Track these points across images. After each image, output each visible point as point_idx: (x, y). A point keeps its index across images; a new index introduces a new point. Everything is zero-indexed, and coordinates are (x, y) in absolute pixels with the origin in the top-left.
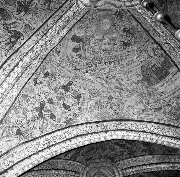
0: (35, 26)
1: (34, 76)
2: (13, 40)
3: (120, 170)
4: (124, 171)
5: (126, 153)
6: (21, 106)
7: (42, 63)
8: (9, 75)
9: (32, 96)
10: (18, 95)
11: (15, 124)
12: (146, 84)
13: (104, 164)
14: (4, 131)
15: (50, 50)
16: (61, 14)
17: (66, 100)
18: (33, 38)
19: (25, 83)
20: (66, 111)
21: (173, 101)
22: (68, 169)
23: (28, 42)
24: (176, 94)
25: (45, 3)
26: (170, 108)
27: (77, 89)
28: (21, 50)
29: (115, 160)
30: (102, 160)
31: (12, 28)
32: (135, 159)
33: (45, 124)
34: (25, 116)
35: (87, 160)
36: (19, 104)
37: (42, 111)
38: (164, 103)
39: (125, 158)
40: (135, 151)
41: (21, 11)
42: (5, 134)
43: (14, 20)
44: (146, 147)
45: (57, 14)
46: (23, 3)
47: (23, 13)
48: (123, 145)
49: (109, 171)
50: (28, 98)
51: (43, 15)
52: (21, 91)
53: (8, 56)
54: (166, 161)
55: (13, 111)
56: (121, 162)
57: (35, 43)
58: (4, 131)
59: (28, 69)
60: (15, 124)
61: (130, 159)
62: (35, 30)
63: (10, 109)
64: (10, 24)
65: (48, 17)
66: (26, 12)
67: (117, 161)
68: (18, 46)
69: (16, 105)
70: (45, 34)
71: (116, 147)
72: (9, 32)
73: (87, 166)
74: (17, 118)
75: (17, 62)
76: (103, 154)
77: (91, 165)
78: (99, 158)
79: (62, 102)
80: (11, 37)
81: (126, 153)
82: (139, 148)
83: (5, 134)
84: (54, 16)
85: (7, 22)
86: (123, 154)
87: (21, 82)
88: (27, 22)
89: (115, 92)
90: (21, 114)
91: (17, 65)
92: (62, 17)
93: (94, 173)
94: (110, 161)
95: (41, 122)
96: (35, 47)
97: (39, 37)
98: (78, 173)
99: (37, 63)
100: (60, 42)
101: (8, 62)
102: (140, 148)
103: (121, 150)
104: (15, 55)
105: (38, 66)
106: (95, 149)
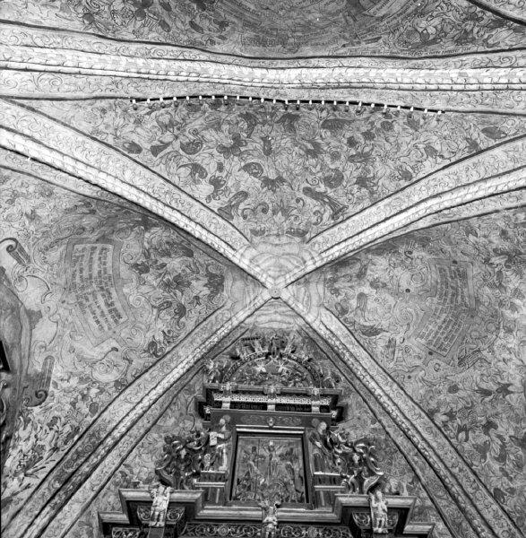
3: (315, 255)
4: (324, 255)
5: (326, 216)
12: (353, 11)
13: (287, 249)
17: (198, 18)
20: (193, 31)
21: (404, 23)
22: (212, 229)
24: (409, 11)
26: (397, 34)
27: (223, 14)
29: (308, 236)
30: (284, 239)
32: (343, 226)
33: (146, 29)
35: (255, 233)
38: (385, 30)
39: (326, 227)
40: (345, 207)
44: (364, 190)
48: (320, 193)
49: (295, 263)
54: (403, 207)
56: (319, 238)
61: (336, 229)
67: (311, 239)
71: (309, 200)
73: (252, 245)
76: (286, 226)
77: (262, 248)
78: (278, 235)
79: (188, 19)
81: (326, 216)
82: (350, 196)
86: (322, 220)
89: (294, 32)
93: (267, 264)
94: (298, 239)
95: (139, 24)
98: (234, 249)
102: (353, 195)
103: (317, 208)
106: (270, 212)
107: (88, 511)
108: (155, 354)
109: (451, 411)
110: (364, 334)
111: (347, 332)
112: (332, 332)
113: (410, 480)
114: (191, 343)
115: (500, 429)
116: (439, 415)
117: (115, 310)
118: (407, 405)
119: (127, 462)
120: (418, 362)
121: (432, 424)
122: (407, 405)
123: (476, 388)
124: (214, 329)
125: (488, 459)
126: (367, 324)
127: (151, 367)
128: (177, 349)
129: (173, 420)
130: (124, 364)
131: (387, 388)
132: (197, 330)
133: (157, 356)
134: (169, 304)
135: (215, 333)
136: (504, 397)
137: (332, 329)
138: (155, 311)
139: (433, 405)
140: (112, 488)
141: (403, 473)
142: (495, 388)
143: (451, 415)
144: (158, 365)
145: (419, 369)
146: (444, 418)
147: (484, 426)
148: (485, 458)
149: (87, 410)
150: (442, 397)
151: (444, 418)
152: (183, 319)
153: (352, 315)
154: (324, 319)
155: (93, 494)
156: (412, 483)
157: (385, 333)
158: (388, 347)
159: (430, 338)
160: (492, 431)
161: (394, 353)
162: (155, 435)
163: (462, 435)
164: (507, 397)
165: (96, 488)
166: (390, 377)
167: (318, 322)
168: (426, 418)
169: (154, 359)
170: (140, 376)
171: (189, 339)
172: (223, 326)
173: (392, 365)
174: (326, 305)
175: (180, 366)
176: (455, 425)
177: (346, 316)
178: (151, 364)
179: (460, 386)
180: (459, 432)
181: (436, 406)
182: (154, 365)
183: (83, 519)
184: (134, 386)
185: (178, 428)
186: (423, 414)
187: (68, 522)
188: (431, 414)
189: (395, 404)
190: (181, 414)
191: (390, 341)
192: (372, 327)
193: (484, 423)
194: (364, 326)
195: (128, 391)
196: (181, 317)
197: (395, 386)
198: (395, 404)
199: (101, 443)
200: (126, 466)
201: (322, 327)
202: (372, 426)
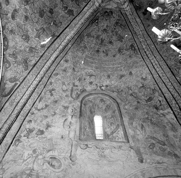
0: (130, 36)
1: (155, 44)
2: (133, 49)
6: (168, 56)
7: (150, 38)
8: (148, 57)
9: (166, 48)
10: (161, 56)
11: (175, 63)
14: (176, 69)
15: (145, 31)
16: (129, 21)
18: (136, 39)
19: (156, 50)
23: (137, 43)
25: (121, 28)
28: (139, 47)
31: (128, 47)
34: (174, 57)
36: (166, 57)
37: (178, 45)
41: (122, 41)
42: (177, 70)
43: (125, 45)
45: (128, 23)
46: (119, 38)
47: (123, 40)
50: (165, 51)
51: (127, 30)
52: (160, 54)
53: (140, 54)
55: (168, 61)
57: (138, 40)
58: (176, 69)
59: (150, 47)
60: (175, 63)
62: (132, 37)
63: (166, 62)
64: (126, 47)
65: (128, 28)
66: (123, 38)
68: (137, 48)
69: (165, 58)
70: (136, 33)
72: (129, 49)
74: (173, 61)
75: (144, 51)
80: (132, 49)
83: (177, 70)
84: (128, 25)
85: (125, 48)
87: (155, 52)
88: (128, 39)
90: (172, 58)
91: (145, 52)
92: (130, 22)
96: (140, 40)
97: (136, 36)
99: (149, 41)
100: (143, 24)
101: (142, 55)
104: (140, 51)
105: (151, 40)
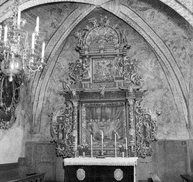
107: (51, 76)
108: (55, 27)
109: (172, 41)
110: (140, 11)
111: (132, 12)
112: (125, 15)
113: (155, 60)
114: (68, 22)
115: (186, 50)
116: (168, 42)
117: (34, 15)
118: (156, 38)
119: (57, 62)
120: (163, 22)
121: (165, 45)
122: (156, 38)
123: (182, 36)
124: (76, 17)
125: (181, 58)
126: (142, 7)
127: (55, 32)
128: (63, 24)
129: (69, 46)
130: (45, 33)
131: (148, 33)
132: (69, 17)
133: (56, 28)
134: (54, 9)
135: (76, 19)
136: (190, 41)
137: (126, 13)
138: (50, 12)
139: (166, 38)
140: (56, 69)
141: (153, 58)
142: (188, 38)
143: (172, 42)
144: (58, 31)
145: (163, 24)
146: (170, 43)
147: (182, 48)
148: (180, 57)
149: (39, 51)
150: (170, 36)
151: (170, 43)
152: (62, 13)
153: (135, 5)
154: (122, 10)
155: (51, 72)
156: (156, 61)
157: (150, 9)
158: (151, 15)
159: (169, 13)
160: (184, 50)
161: (154, 17)
162: (64, 52)
163: (174, 49)
164: (190, 41)
165: (51, 71)
166: (151, 28)
167: (119, 13)
168: (163, 43)
169: (55, 29)
170: (52, 37)
171: (66, 20)
172: (79, 16)
173: (152, 23)
174: (122, 3)
175: (66, 32)
176: (173, 46)
177: (132, 5)
178: (55, 31)
179: (177, 33)
180: (174, 48)
181: (167, 39)
182: (56, 31)
183: (51, 78)
184: (51, 40)
185: (71, 48)
186: (162, 42)
187: (47, 80)
188: (164, 42)
189: (151, 39)
190: (71, 43)
191: (152, 13)
192: (144, 8)
193: (182, 47)
194: (141, 8)
195: (50, 42)
196: (61, 13)
197: (152, 32)
198: (151, 39)
199: (48, 60)
200: (58, 63)
201: (121, 15)
202: (144, 43)
